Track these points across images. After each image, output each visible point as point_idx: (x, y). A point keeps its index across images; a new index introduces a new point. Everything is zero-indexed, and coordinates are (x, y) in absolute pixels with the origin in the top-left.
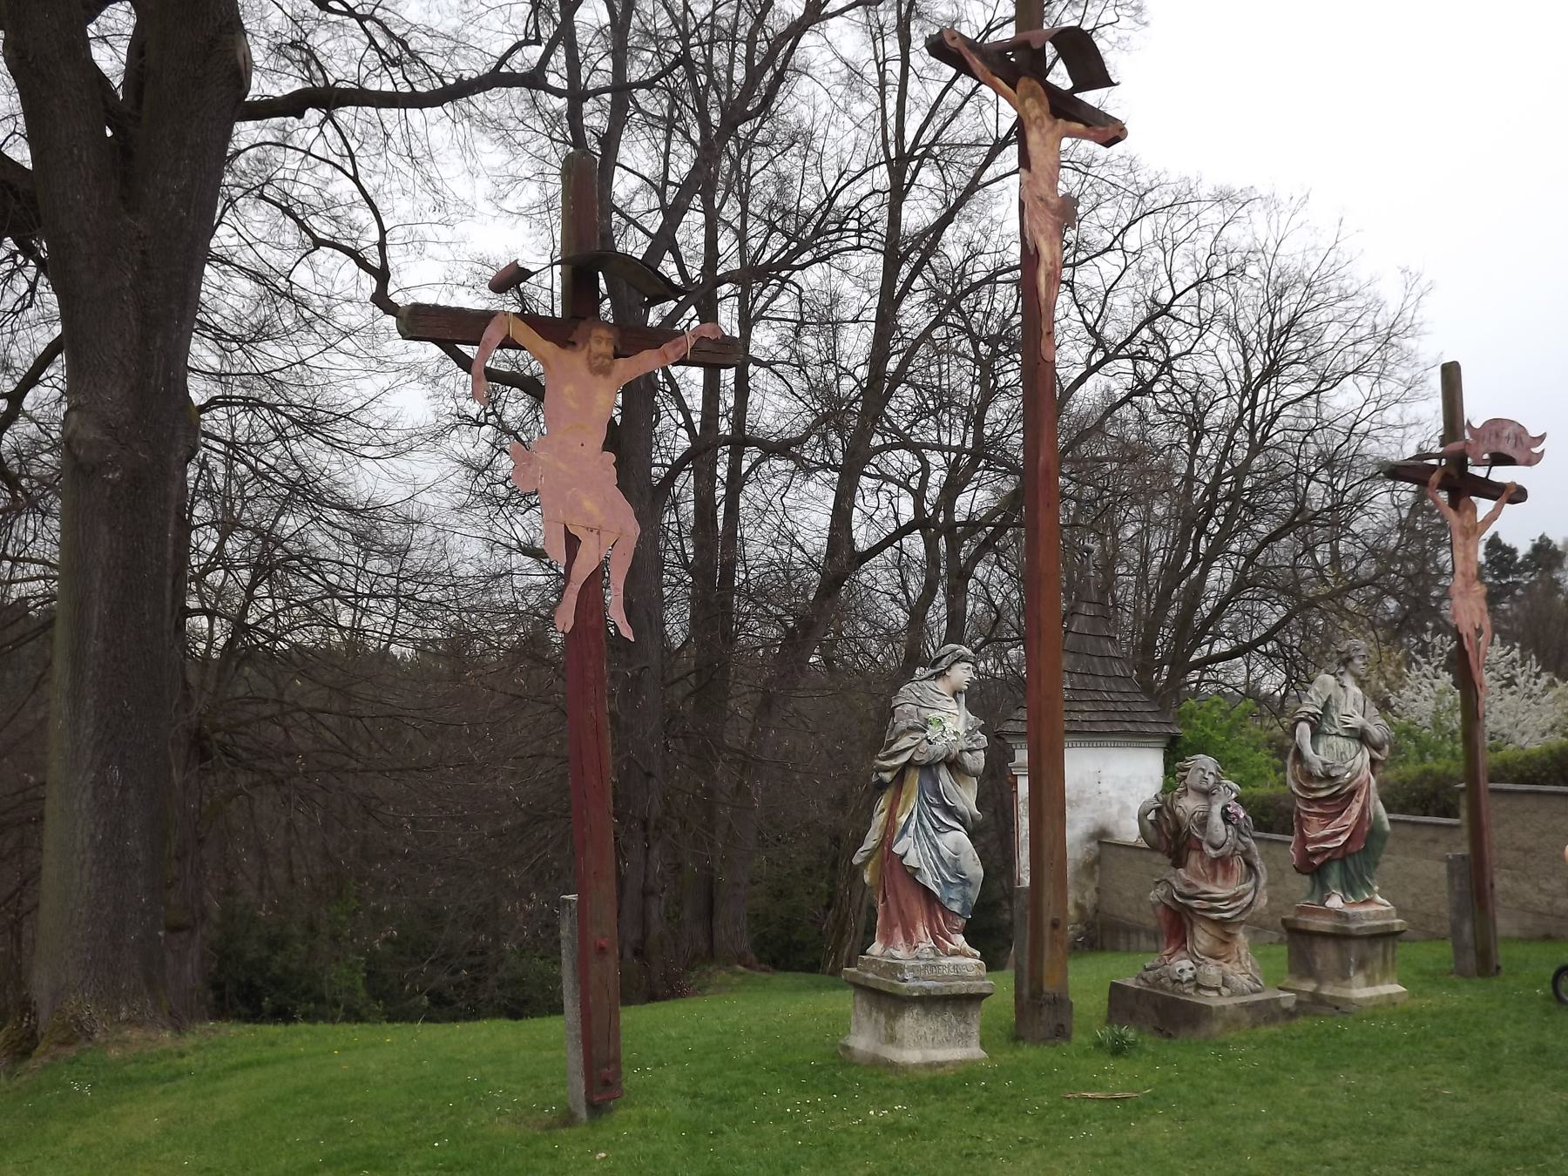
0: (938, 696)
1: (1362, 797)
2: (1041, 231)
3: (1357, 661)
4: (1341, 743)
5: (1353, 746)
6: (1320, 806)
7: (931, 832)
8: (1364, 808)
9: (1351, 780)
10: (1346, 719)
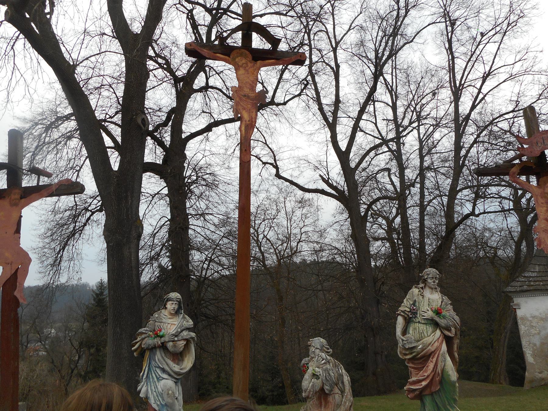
0: (164, 317)
1: (435, 359)
2: (244, 109)
3: (429, 281)
4: (422, 327)
5: (430, 329)
6: (413, 363)
7: (156, 379)
8: (436, 365)
9: (423, 349)
10: (423, 314)
